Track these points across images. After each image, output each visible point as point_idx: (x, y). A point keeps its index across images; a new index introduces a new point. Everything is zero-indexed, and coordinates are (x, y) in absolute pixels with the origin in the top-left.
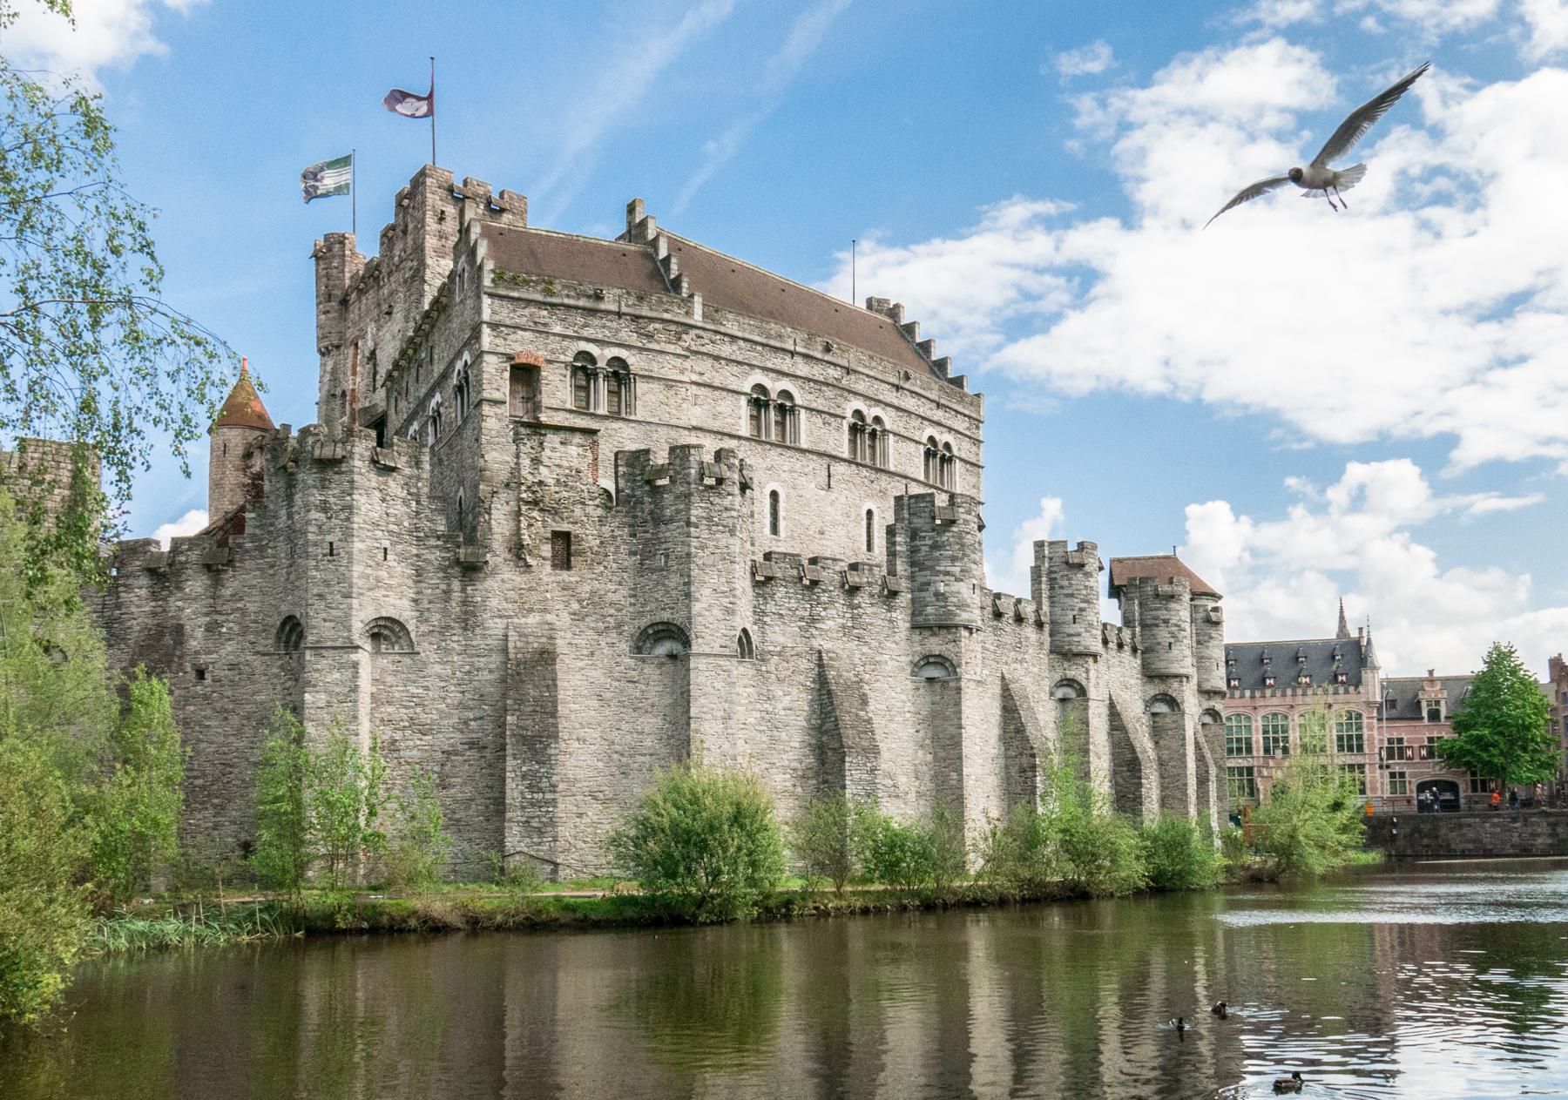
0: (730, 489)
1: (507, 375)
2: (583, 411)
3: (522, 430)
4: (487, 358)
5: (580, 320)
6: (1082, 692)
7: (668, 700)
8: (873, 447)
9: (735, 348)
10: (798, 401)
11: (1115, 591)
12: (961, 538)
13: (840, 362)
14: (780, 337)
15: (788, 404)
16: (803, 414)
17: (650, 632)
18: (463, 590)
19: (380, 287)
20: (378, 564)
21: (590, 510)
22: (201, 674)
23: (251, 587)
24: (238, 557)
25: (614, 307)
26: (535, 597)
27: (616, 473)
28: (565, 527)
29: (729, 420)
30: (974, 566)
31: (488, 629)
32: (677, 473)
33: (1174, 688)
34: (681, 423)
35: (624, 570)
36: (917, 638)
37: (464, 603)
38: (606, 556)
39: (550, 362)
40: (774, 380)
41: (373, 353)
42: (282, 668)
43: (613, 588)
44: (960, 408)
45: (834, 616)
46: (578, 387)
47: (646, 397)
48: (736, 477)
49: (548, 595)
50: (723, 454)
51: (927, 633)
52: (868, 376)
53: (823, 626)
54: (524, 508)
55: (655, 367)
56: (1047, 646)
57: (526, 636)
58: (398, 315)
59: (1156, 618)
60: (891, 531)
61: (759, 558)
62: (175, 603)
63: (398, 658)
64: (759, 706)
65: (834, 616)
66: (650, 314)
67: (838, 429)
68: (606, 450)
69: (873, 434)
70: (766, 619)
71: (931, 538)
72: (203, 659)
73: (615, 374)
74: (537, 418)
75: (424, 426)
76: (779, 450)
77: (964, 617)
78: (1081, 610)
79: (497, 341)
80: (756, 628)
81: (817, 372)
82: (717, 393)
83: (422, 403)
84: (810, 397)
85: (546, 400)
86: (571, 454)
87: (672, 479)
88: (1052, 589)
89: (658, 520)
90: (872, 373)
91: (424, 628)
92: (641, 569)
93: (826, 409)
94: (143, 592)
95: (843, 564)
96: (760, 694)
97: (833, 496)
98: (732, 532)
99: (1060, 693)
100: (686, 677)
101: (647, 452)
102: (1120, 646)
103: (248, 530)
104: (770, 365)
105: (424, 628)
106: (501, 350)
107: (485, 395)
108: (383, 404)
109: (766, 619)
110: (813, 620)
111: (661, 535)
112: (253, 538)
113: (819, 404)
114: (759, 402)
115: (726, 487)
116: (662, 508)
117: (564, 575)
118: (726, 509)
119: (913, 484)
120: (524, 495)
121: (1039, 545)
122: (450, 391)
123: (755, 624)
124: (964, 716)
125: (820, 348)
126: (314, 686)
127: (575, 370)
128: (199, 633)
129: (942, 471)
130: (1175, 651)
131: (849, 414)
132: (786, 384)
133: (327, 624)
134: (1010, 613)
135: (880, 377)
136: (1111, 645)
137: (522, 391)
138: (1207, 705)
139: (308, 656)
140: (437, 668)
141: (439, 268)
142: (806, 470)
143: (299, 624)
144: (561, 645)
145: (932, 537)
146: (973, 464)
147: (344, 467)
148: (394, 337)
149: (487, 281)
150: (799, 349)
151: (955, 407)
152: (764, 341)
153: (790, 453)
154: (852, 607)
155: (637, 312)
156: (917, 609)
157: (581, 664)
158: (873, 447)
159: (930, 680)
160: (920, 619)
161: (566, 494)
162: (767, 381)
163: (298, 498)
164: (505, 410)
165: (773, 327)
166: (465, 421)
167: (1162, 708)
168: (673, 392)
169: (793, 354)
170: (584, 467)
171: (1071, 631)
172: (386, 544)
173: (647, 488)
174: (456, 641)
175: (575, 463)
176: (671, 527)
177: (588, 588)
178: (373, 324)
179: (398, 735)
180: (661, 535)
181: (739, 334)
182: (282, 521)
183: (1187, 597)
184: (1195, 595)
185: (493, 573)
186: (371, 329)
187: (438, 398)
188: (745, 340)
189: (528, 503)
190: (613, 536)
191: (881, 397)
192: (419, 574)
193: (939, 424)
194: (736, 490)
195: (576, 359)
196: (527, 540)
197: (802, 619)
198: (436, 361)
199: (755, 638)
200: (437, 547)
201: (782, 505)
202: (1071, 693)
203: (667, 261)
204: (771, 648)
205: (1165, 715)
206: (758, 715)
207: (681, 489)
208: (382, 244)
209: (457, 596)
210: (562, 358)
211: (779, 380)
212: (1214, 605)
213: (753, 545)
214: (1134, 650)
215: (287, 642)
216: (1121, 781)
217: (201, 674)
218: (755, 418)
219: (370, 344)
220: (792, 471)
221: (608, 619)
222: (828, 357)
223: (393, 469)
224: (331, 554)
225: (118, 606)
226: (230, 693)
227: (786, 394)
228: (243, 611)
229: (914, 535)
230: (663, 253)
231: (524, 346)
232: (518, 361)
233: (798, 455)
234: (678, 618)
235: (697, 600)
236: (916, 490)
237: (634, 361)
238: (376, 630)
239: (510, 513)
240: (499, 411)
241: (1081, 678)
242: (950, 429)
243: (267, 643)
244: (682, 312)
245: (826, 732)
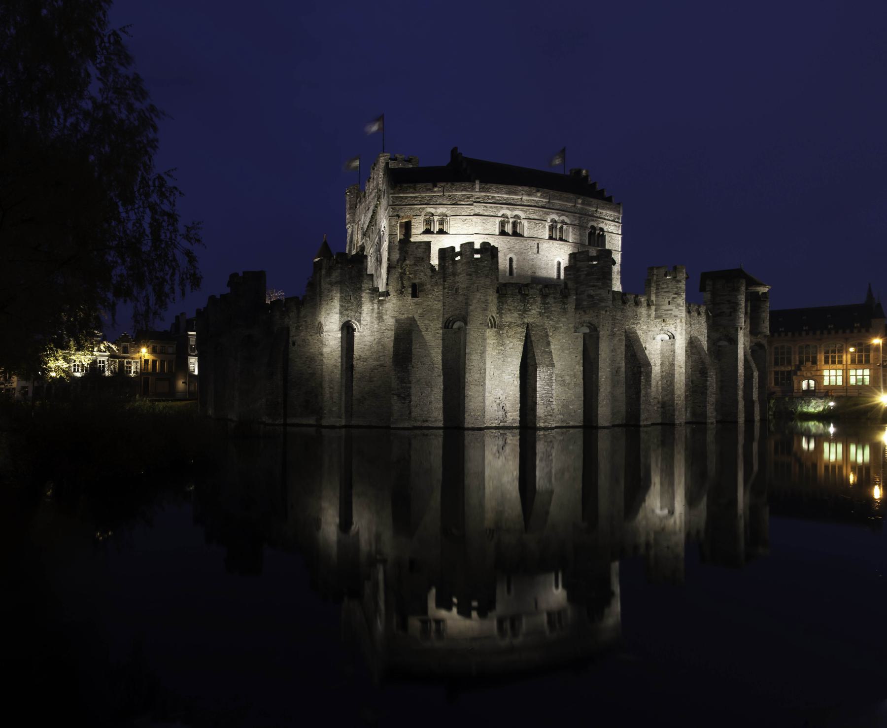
38: (434, 290)
43: (436, 302)
70: (503, 311)
80: (498, 315)
96: (498, 343)
109: (503, 311)
110: (525, 311)
117: (416, 299)
123: (497, 314)
126: (327, 346)
136: (693, 314)
154: (544, 303)
171: (667, 309)
197: (520, 310)
199: (497, 320)
204: (504, 324)
239: (398, 278)
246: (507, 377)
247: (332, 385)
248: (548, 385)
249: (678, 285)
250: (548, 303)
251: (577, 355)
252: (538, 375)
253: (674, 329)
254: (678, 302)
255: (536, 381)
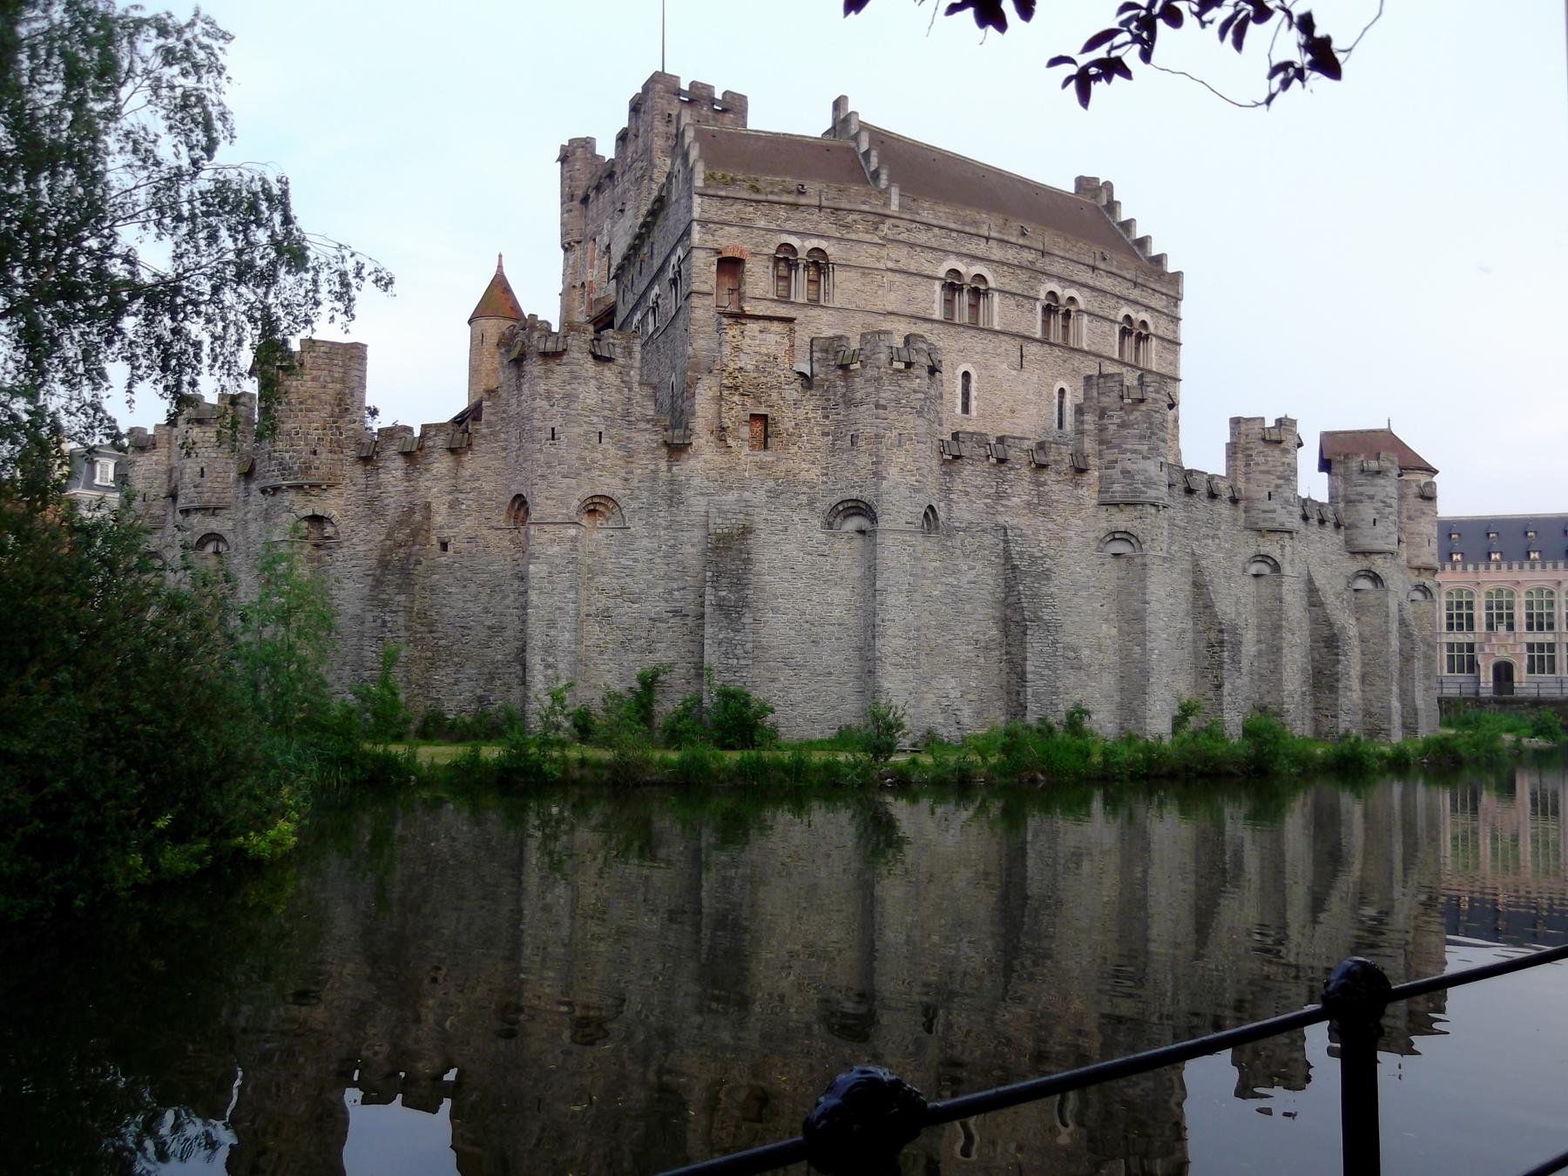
0: (917, 372)
1: (714, 268)
2: (784, 299)
3: (725, 321)
4: (695, 253)
5: (783, 214)
6: (1276, 568)
7: (857, 573)
8: (1066, 327)
9: (930, 234)
10: (992, 284)
11: (1325, 465)
12: (1150, 417)
13: (1035, 245)
14: (974, 223)
15: (982, 287)
16: (996, 298)
17: (841, 508)
18: (670, 470)
19: (615, 186)
20: (593, 447)
21: (786, 394)
22: (444, 546)
23: (487, 468)
24: (475, 442)
25: (815, 202)
26: (733, 476)
27: (811, 359)
28: (762, 410)
29: (923, 304)
30: (1162, 444)
31: (689, 506)
32: (868, 358)
33: (1379, 565)
34: (875, 309)
35: (817, 450)
36: (1103, 514)
37: (671, 482)
38: (801, 436)
39: (755, 254)
40: (968, 265)
41: (608, 247)
42: (512, 541)
43: (807, 466)
44: (1157, 287)
45: (1021, 490)
46: (780, 278)
47: (843, 285)
48: (924, 360)
49: (747, 474)
50: (911, 339)
51: (1113, 510)
52: (1062, 258)
53: (1009, 503)
54: (725, 393)
55: (853, 256)
56: (1241, 522)
57: (724, 512)
58: (629, 213)
59: (1361, 494)
60: (1079, 411)
61: (948, 438)
62: (424, 483)
63: (611, 532)
64: (943, 579)
65: (1021, 490)
66: (848, 207)
67: (1032, 310)
68: (803, 336)
69: (1067, 314)
71: (1120, 417)
72: (446, 533)
73: (816, 263)
74: (742, 308)
75: (645, 316)
76: (972, 332)
77: (1152, 494)
78: (1278, 486)
79: (706, 237)
80: (942, 504)
81: (1010, 255)
82: (913, 279)
83: (644, 294)
84: (1003, 279)
85: (749, 290)
86: (770, 340)
87: (863, 366)
88: (1248, 465)
89: (849, 402)
90: (1067, 255)
91: (634, 505)
92: (833, 450)
93: (1020, 292)
94: (399, 474)
95: (1029, 442)
97: (1025, 375)
98: (920, 413)
99: (1254, 569)
100: (873, 551)
101: (840, 338)
102: (1322, 522)
103: (484, 417)
104: (964, 251)
105: (634, 505)
106: (710, 245)
107: (694, 287)
108: (614, 294)
110: (1000, 496)
111: (852, 417)
112: (489, 424)
113: (1013, 286)
114: (952, 286)
115: (915, 371)
116: (853, 392)
118: (915, 391)
119: (1107, 362)
120: (725, 381)
121: (1236, 422)
122: (666, 283)
124: (1148, 591)
125: (1015, 233)
126: (538, 558)
127: (777, 261)
128: (444, 509)
129: (1137, 349)
130: (1379, 528)
131: (1042, 295)
132: (978, 269)
133: (549, 502)
134: (1203, 490)
135: (1075, 258)
137: (728, 283)
138: (1416, 580)
139: (533, 530)
140: (645, 542)
141: (663, 164)
142: (999, 351)
143: (525, 502)
144: (758, 521)
145: (1120, 417)
146: (1170, 341)
147: (565, 359)
148: (626, 233)
149: (699, 182)
150: (993, 234)
151: (1153, 286)
152: (960, 228)
153: (983, 335)
155: (837, 206)
156: (1105, 485)
157: (776, 538)
158: (1066, 327)
159: (1116, 555)
160: (1107, 497)
161: (763, 379)
162: (961, 268)
163: (525, 388)
164: (710, 301)
165: (970, 213)
166: (677, 312)
167: (1364, 584)
168: (869, 280)
169: (987, 239)
170: (781, 354)
171: (1266, 508)
172: (602, 428)
173: (840, 372)
174: (662, 517)
175: (773, 350)
176: (861, 409)
177: (782, 467)
178: (608, 221)
179: (611, 603)
180: (852, 417)
181: (934, 222)
182: (513, 410)
183: (1395, 472)
184: (1403, 470)
185: (696, 455)
186: (607, 225)
187: (656, 290)
188: (941, 228)
189: (729, 388)
190: (807, 419)
191: (1075, 278)
192: (630, 455)
193: (1136, 303)
194: (925, 373)
195: (777, 252)
196: (727, 422)
197: (987, 497)
198: (655, 256)
199: (941, 515)
200: (646, 430)
201: (973, 385)
202: (1265, 569)
203: (867, 154)
204: (957, 524)
205: (1368, 591)
206: (944, 589)
207: (870, 372)
208: (617, 146)
209: (664, 475)
210: (766, 250)
211: (972, 265)
212: (1428, 480)
213: (940, 425)
214: (1337, 526)
215: (516, 518)
216: (1317, 657)
217: (444, 546)
218: (949, 302)
219: (606, 240)
220: (984, 352)
221: (801, 497)
222: (1021, 241)
223: (610, 360)
224: (553, 439)
225: (378, 486)
226: (468, 564)
227: (980, 277)
228: (480, 491)
229: (1103, 413)
230: (864, 146)
231: (731, 241)
232: (725, 255)
233: (991, 337)
234: (867, 496)
235: (884, 478)
236: (1110, 369)
237: (831, 249)
238: (591, 507)
240: (707, 303)
241: (1276, 555)
242: (1147, 308)
243: (500, 519)
244: (880, 203)
245: (1007, 606)
246: (963, 648)
247: (551, 660)
248: (1048, 667)
249: (1285, 460)
250: (1044, 484)
251: (1103, 602)
252: (1028, 646)
253: (1279, 551)
254: (1285, 495)
255: (1025, 659)
